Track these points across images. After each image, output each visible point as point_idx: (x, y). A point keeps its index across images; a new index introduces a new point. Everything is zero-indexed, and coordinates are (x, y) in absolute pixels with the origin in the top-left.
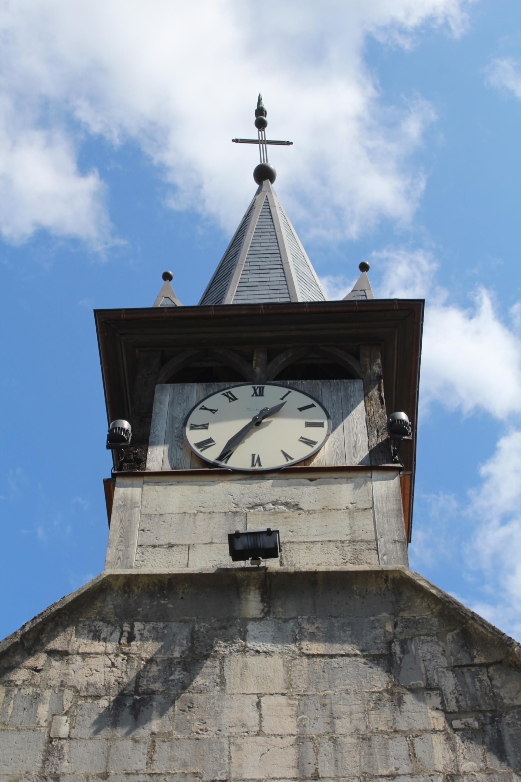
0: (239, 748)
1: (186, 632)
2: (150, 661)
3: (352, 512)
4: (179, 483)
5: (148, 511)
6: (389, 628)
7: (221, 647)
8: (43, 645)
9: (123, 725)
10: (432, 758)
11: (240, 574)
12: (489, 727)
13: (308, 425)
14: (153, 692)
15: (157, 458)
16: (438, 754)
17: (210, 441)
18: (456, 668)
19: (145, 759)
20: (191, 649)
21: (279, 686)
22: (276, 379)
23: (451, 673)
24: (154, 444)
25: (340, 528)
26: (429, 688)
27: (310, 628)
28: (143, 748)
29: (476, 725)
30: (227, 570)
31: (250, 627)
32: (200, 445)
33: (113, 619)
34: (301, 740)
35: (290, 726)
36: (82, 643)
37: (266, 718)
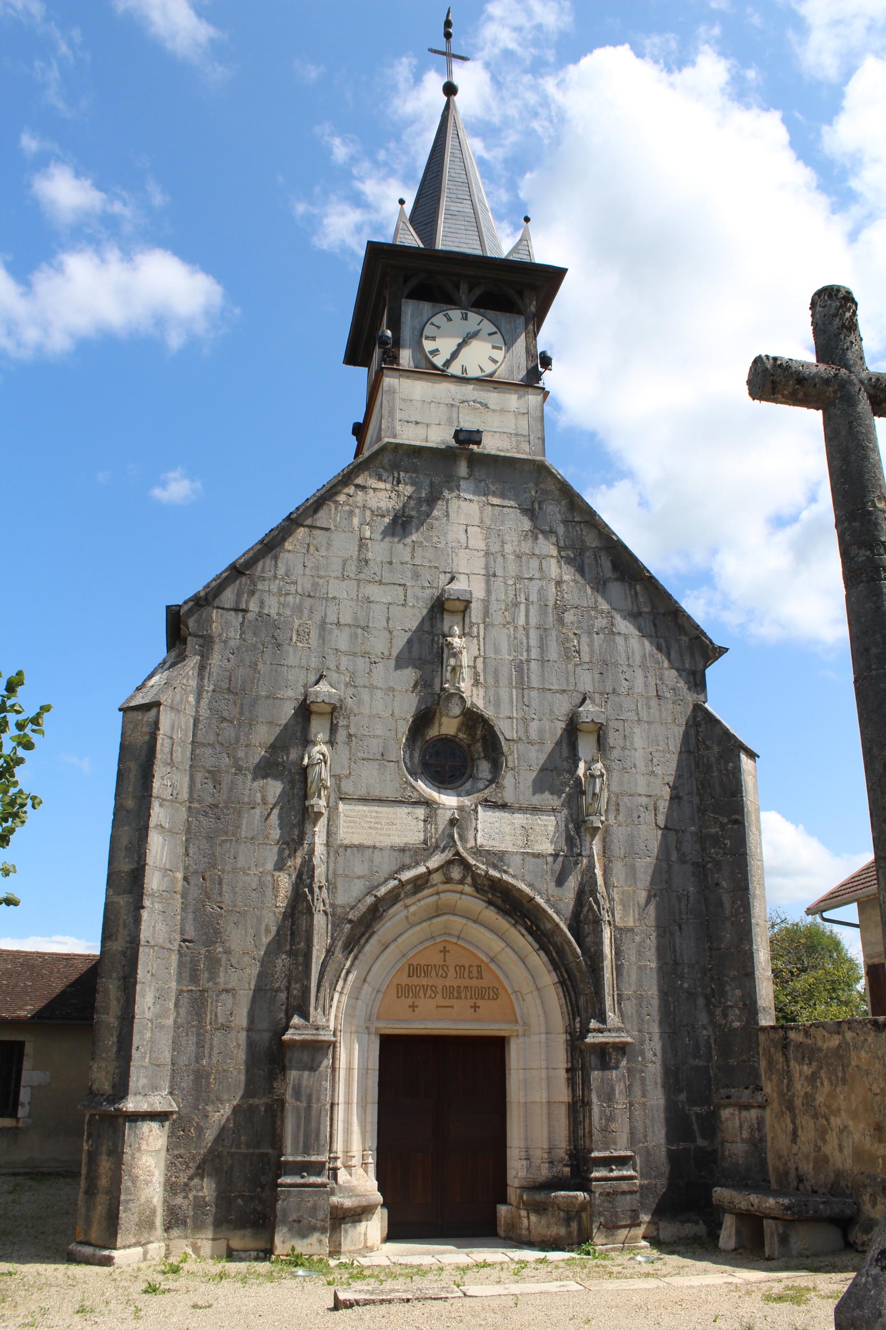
0: (457, 555)
1: (428, 482)
2: (410, 497)
3: (517, 414)
4: (420, 379)
5: (403, 397)
6: (533, 493)
7: (446, 494)
8: (352, 481)
9: (398, 536)
10: (550, 571)
11: (458, 451)
12: (578, 558)
13: (494, 347)
14: (412, 517)
15: (406, 357)
16: (553, 569)
17: (437, 350)
18: (565, 522)
19: (410, 555)
20: (431, 492)
21: (477, 523)
22: (472, 307)
23: (562, 525)
24: (404, 347)
25: (510, 424)
26: (551, 532)
27: (493, 488)
28: (409, 549)
29: (572, 555)
30: (451, 447)
31: (462, 483)
32: (432, 352)
33: (388, 468)
34: (487, 554)
35: (482, 545)
36: (372, 482)
37: (470, 539)
